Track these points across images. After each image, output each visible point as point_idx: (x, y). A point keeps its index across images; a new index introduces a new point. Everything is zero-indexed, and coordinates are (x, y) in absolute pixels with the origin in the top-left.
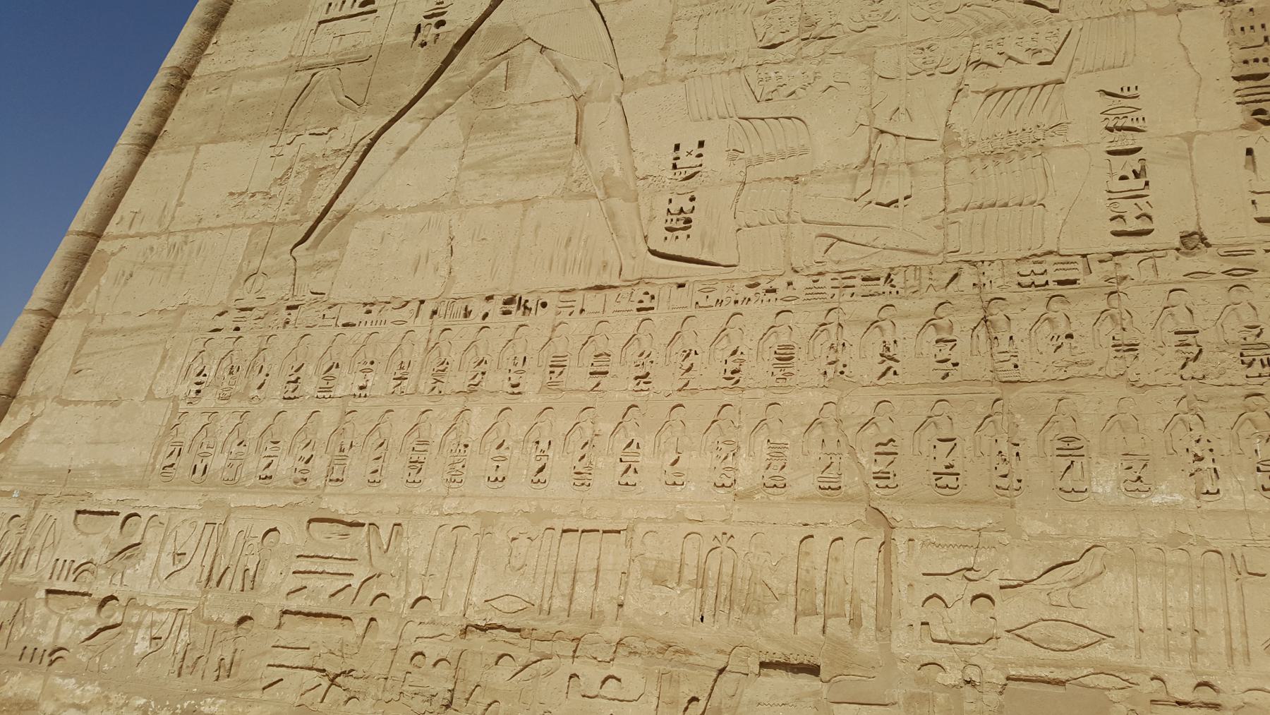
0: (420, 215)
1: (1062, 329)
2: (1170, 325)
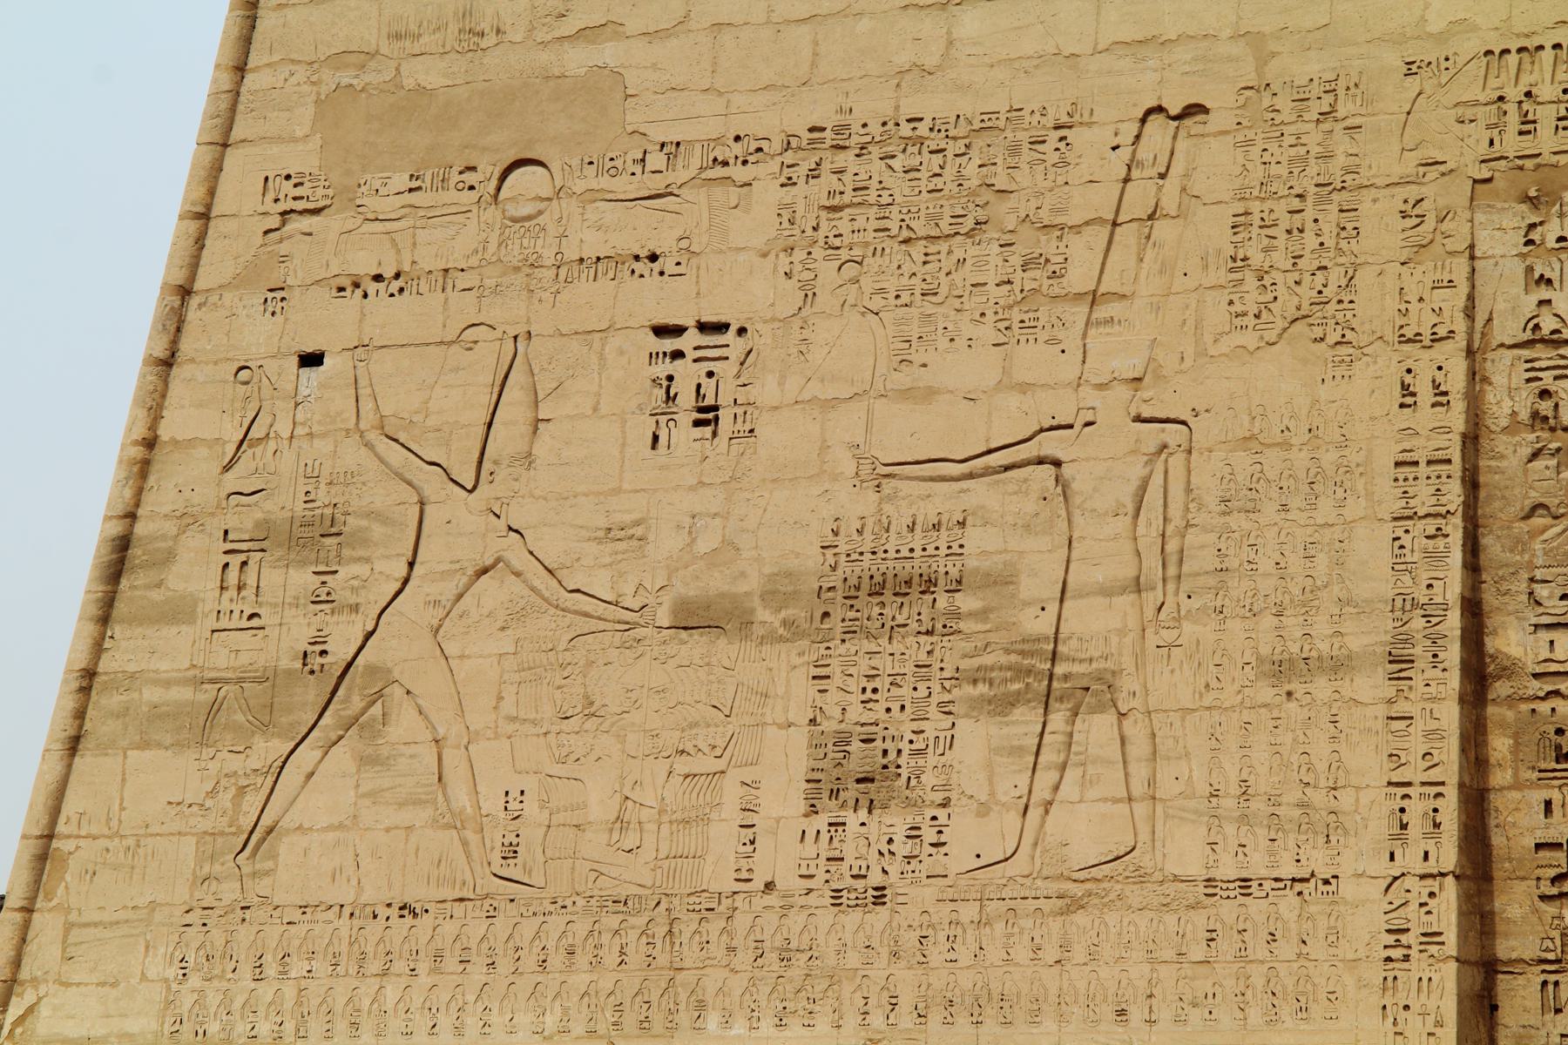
0: (331, 834)
1: (704, 939)
2: (752, 937)
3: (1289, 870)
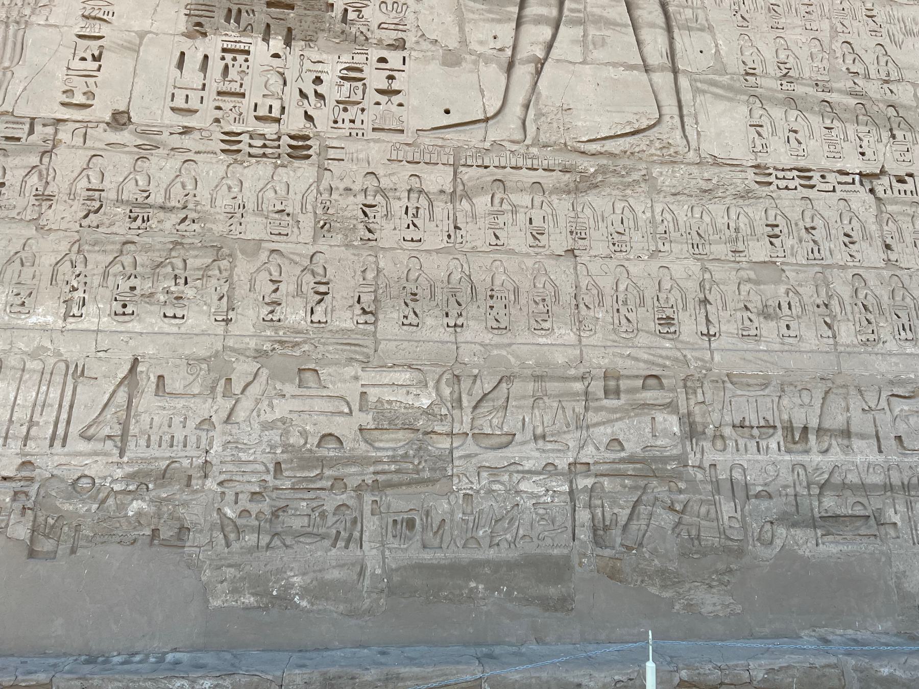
3: (854, 164)
